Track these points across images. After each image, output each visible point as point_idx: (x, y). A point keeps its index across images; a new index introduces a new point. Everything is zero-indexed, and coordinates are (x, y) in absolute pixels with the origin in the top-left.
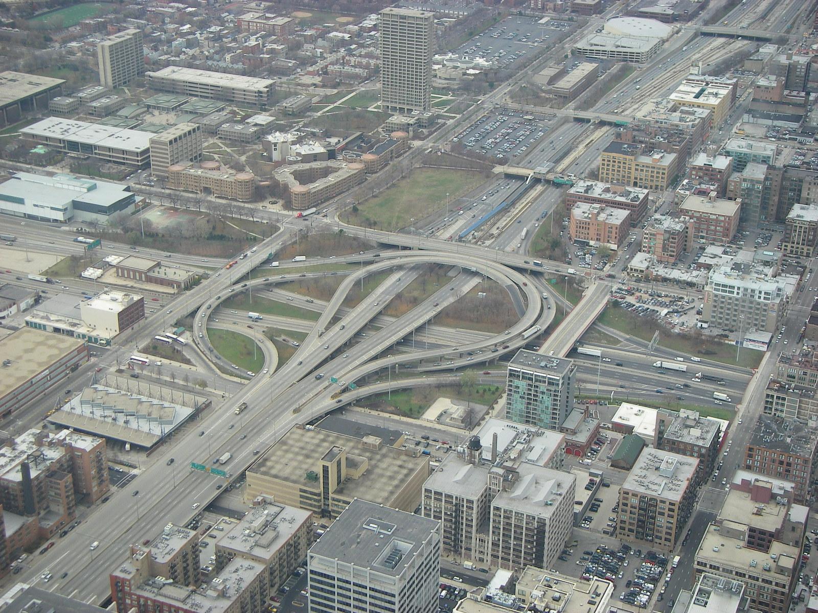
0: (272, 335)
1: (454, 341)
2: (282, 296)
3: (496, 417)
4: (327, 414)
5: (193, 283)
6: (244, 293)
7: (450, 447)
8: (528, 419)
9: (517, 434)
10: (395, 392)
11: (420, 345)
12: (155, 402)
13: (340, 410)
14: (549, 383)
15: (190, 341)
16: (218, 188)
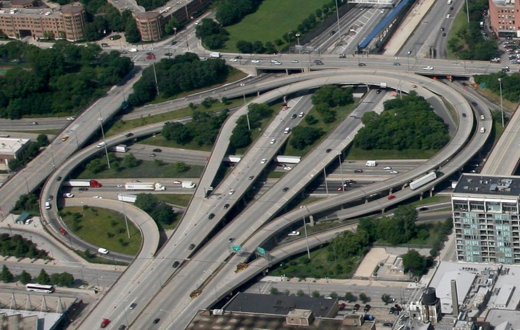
0: (147, 203)
1: (376, 173)
2: (143, 151)
3: (446, 259)
4: (235, 291)
5: (27, 154)
6: (99, 155)
7: (396, 306)
8: (485, 254)
9: (476, 277)
10: (314, 249)
11: (335, 187)
12: (9, 312)
13: (255, 280)
14: (504, 209)
15: (40, 229)
16: (40, 29)
